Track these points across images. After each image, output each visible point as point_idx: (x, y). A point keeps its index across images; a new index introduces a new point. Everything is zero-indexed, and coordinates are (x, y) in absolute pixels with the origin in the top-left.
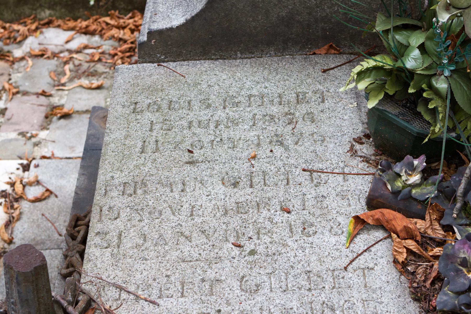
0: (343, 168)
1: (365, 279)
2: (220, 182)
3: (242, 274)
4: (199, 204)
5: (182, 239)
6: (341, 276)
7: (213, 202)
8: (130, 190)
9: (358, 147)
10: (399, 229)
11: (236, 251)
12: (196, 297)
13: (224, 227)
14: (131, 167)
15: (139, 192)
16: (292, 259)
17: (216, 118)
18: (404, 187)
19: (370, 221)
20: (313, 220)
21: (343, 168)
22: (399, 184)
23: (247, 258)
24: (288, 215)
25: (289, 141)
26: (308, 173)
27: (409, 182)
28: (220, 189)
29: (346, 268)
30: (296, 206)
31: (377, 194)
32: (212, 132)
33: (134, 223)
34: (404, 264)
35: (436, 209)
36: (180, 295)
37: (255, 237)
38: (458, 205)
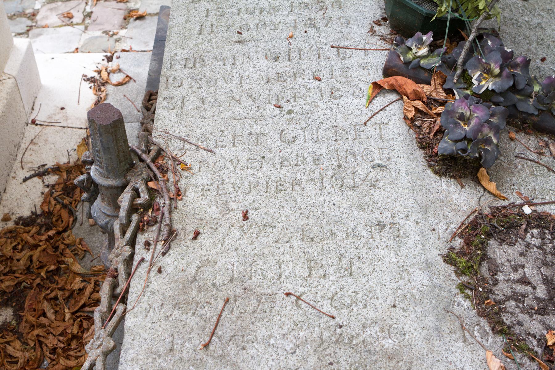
0: (364, 45)
1: (380, 132)
2: (264, 57)
3: (281, 129)
4: (247, 74)
5: (233, 102)
6: (361, 130)
7: (258, 73)
8: (190, 64)
9: (376, 28)
10: (409, 92)
11: (277, 111)
12: (244, 146)
13: (267, 92)
14: (191, 46)
15: (198, 65)
16: (322, 117)
17: (260, 6)
18: (414, 59)
19: (386, 86)
20: (339, 86)
21: (364, 45)
22: (410, 56)
23: (285, 116)
24: (319, 82)
25: (320, 24)
26: (336, 49)
27: (418, 54)
28: (264, 63)
29: (365, 124)
30: (325, 75)
31: (392, 65)
32: (257, 17)
33: (194, 90)
34: (413, 120)
35: (440, 75)
36: (232, 145)
37: (292, 100)
38: (458, 72)
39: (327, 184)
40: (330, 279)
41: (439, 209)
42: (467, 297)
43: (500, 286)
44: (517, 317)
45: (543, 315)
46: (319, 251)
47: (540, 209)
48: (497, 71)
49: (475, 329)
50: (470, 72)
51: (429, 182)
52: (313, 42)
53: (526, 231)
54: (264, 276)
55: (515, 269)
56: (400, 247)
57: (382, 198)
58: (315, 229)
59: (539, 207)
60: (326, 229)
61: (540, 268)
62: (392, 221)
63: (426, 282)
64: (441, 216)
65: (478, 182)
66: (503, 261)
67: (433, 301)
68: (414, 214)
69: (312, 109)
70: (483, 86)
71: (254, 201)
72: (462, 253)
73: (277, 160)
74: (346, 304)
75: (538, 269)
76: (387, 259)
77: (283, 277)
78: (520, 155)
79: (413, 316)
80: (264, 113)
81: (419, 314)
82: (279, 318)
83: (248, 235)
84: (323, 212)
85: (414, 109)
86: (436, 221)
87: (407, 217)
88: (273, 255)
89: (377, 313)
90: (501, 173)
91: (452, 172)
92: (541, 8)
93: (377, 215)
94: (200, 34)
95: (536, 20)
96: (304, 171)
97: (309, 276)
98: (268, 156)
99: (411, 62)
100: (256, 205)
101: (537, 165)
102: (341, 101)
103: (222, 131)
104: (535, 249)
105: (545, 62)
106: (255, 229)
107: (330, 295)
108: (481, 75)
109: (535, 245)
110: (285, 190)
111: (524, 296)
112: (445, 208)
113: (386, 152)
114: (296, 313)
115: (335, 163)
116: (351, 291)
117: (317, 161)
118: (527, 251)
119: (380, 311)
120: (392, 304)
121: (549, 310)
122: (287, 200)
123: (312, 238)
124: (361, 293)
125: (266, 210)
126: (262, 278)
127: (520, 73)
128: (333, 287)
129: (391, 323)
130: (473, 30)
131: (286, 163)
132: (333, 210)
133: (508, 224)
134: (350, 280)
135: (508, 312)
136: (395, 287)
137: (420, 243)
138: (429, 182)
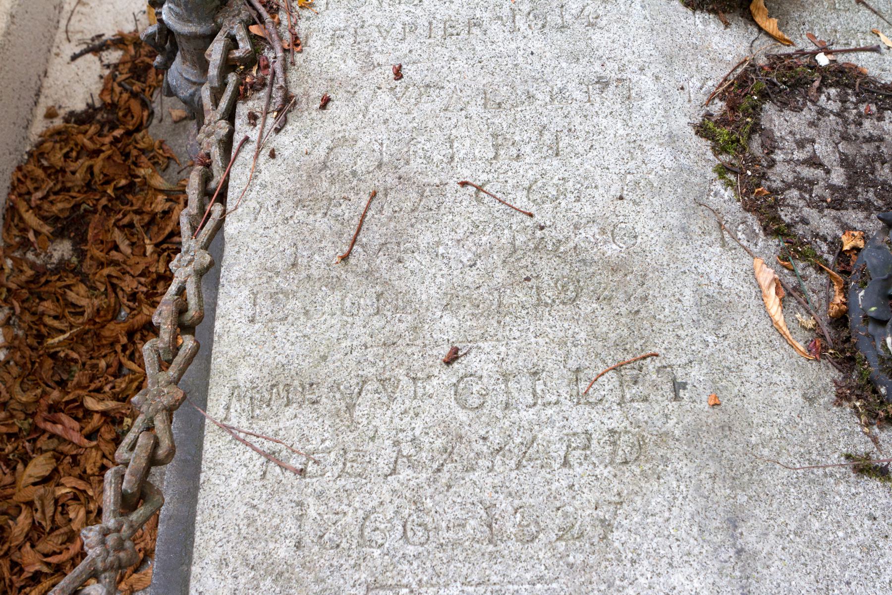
39: (521, 23)
40: (527, 161)
41: (690, 58)
42: (729, 184)
43: (778, 168)
44: (800, 212)
46: (510, 122)
47: (841, 59)
49: (740, 228)
53: (819, 90)
54: (428, 159)
55: (801, 144)
57: (604, 43)
58: (504, 90)
61: (837, 144)
62: (619, 76)
63: (668, 163)
64: (694, 68)
68: (653, 66)
71: (410, 51)
72: (723, 121)
74: (550, 196)
76: (612, 132)
77: (456, 159)
79: (648, 210)
81: (658, 208)
82: (451, 217)
84: (516, 65)
86: (686, 76)
89: (596, 208)
93: (597, 67)
96: (486, 4)
97: (495, 158)
104: (832, 117)
107: (526, 184)
109: (831, 112)
110: (458, 34)
111: (812, 183)
112: (700, 57)
114: (476, 209)
116: (557, 177)
118: (819, 119)
119: (601, 204)
120: (618, 194)
122: (460, 49)
123: (499, 104)
124: (572, 180)
125: (429, 64)
126: (425, 162)
129: (616, 221)
132: (530, 62)
133: (793, 80)
134: (555, 162)
135: (788, 205)
136: (623, 171)
137: (661, 107)
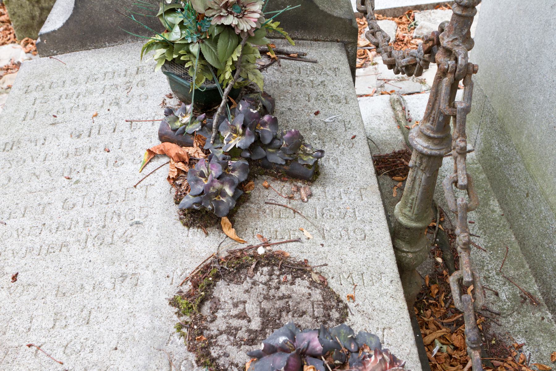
0: (154, 117)
1: (146, 192)
2: (69, 136)
3: (66, 198)
4: (51, 152)
5: (34, 178)
6: (131, 192)
7: (61, 150)
8: (8, 148)
9: (168, 100)
10: (173, 155)
11: (67, 181)
12: (32, 216)
13: (63, 166)
14: (13, 131)
15: (14, 148)
16: (102, 184)
17: (79, 91)
18: (181, 126)
19: (157, 152)
20: (123, 155)
21: (154, 117)
22: (178, 124)
23: (73, 186)
24: (108, 153)
25: (123, 103)
26: (130, 123)
27: (183, 122)
28: (68, 139)
29: (135, 186)
30: (115, 147)
31: (163, 133)
32: (73, 101)
33: (5, 170)
34: (174, 179)
35: (199, 138)
36: (22, 215)
37: (81, 172)
38: (214, 134)
39: (89, 244)
40: (69, 329)
41: (179, 257)
42: (183, 335)
43: (217, 322)
44: (225, 349)
45: (250, 345)
46: (67, 304)
47: (275, 248)
48: (241, 131)
49: (183, 363)
50: (222, 133)
51: (176, 234)
52: (113, 118)
53: (256, 270)
54: (16, 331)
55: (236, 305)
56: (134, 294)
57: (131, 252)
58: (69, 285)
59: (275, 246)
60: (79, 283)
61: (261, 303)
62: (134, 272)
63: (147, 325)
64: (179, 263)
65: (220, 228)
66: (226, 299)
67: (149, 342)
68: (154, 264)
69: (95, 178)
70: (230, 145)
71: (26, 264)
72: (189, 295)
73: (54, 226)
74: (76, 350)
75: (258, 303)
76: (121, 307)
77: (31, 330)
78: (270, 202)
79: (128, 356)
80: (56, 185)
81: (134, 354)
82: (18, 367)
83: (13, 295)
84: (80, 269)
85: (176, 170)
86: (173, 268)
87: (147, 267)
88: (28, 311)
89: (100, 357)
90: (248, 219)
91: (199, 222)
92: (328, 68)
93: (123, 268)
94: (24, 120)
95: (320, 79)
96: (74, 233)
97: (53, 328)
98: (48, 222)
99: (177, 129)
100: (27, 267)
101: (284, 208)
102: (121, 169)
103: (17, 204)
104: (261, 286)
105: (319, 115)
106: (20, 289)
107: (65, 343)
108: (231, 135)
109: (261, 283)
110: (54, 252)
111: (237, 329)
112: (185, 256)
113: (145, 210)
114: (33, 361)
115: (101, 224)
116: (83, 338)
117: (87, 223)
118: (252, 288)
119: (102, 355)
120: (114, 347)
121: (258, 340)
122: (52, 261)
123: (64, 294)
124: (90, 339)
125: (33, 272)
126: (14, 332)
127: (269, 129)
128: (69, 335)
129: (108, 364)
130: (223, 97)
131: (60, 228)
132: (87, 266)
133: (238, 265)
134: (85, 328)
135: (218, 345)
136: (120, 332)
137: (152, 289)
138: (176, 234)
